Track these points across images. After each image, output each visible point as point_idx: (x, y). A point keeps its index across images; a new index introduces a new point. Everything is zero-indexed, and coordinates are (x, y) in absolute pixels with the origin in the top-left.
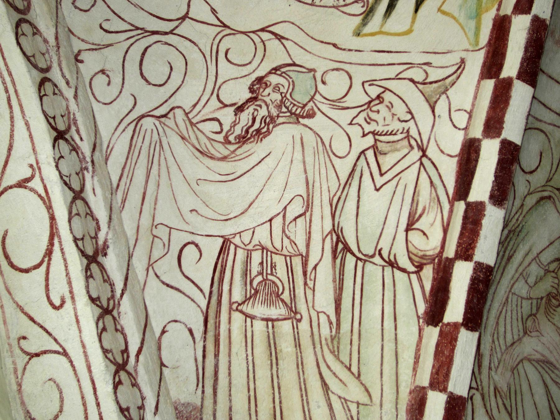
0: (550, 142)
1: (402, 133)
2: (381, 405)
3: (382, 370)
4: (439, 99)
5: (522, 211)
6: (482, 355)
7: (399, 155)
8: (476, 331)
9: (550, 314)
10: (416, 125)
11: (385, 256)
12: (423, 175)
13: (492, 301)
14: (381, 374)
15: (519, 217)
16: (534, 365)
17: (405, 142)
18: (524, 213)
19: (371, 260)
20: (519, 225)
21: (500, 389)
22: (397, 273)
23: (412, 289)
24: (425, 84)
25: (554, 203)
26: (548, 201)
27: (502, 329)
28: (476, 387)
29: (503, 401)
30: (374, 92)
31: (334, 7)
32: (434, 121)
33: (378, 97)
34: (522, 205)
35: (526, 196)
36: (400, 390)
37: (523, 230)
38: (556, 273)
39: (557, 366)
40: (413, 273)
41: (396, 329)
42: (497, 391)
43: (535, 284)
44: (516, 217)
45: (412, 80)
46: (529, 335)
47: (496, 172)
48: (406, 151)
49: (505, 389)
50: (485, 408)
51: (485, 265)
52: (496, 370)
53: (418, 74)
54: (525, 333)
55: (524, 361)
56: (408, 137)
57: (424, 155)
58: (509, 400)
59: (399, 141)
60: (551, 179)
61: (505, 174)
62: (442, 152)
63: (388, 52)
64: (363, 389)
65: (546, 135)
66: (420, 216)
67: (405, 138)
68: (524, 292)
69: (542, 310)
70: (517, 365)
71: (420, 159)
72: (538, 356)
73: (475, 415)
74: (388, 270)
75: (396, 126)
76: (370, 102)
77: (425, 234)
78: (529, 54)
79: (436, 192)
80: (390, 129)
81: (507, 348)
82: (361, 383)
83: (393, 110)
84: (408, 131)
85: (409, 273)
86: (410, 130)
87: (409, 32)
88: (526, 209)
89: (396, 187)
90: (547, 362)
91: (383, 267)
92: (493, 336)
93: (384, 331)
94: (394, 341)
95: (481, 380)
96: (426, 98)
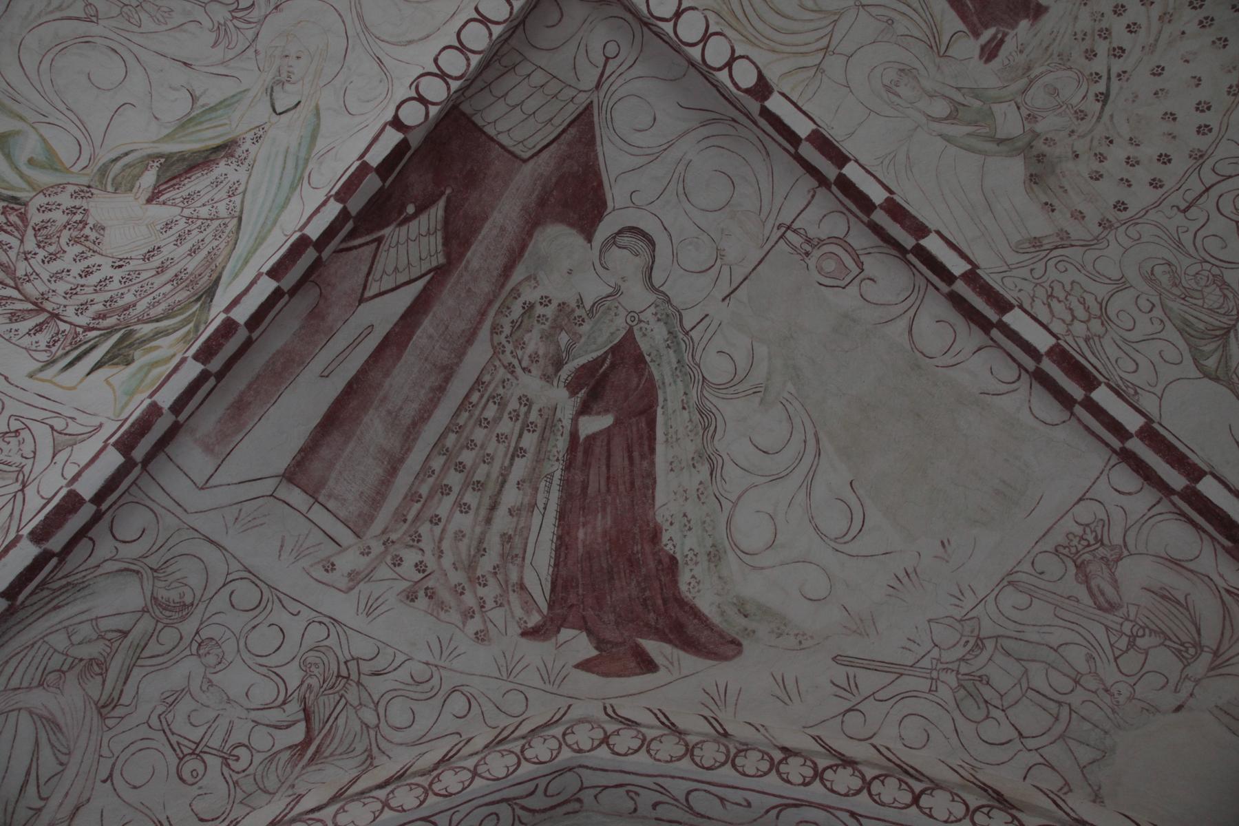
0: (158, 523)
9: (84, 677)
18: (96, 574)
20: (83, 582)
24: (60, 433)
26: (135, 575)
30: (15, 425)
31: (26, 349)
33: (17, 431)
34: (98, 566)
35: (107, 560)
38: (112, 643)
39: (64, 729)
43: (79, 644)
44: (84, 573)
45: (52, 427)
46: (44, 688)
47: (48, 514)
48: (11, 482)
53: (59, 424)
54: (40, 684)
56: (21, 471)
57: (22, 491)
62: (38, 492)
63: (47, 398)
65: (156, 516)
68: (61, 647)
72: (46, 713)
75: (17, 459)
76: (7, 433)
78: (133, 430)
79: (10, 523)
80: (9, 460)
83: (21, 447)
84: (23, 467)
87: (74, 388)
88: (100, 571)
90: (53, 722)
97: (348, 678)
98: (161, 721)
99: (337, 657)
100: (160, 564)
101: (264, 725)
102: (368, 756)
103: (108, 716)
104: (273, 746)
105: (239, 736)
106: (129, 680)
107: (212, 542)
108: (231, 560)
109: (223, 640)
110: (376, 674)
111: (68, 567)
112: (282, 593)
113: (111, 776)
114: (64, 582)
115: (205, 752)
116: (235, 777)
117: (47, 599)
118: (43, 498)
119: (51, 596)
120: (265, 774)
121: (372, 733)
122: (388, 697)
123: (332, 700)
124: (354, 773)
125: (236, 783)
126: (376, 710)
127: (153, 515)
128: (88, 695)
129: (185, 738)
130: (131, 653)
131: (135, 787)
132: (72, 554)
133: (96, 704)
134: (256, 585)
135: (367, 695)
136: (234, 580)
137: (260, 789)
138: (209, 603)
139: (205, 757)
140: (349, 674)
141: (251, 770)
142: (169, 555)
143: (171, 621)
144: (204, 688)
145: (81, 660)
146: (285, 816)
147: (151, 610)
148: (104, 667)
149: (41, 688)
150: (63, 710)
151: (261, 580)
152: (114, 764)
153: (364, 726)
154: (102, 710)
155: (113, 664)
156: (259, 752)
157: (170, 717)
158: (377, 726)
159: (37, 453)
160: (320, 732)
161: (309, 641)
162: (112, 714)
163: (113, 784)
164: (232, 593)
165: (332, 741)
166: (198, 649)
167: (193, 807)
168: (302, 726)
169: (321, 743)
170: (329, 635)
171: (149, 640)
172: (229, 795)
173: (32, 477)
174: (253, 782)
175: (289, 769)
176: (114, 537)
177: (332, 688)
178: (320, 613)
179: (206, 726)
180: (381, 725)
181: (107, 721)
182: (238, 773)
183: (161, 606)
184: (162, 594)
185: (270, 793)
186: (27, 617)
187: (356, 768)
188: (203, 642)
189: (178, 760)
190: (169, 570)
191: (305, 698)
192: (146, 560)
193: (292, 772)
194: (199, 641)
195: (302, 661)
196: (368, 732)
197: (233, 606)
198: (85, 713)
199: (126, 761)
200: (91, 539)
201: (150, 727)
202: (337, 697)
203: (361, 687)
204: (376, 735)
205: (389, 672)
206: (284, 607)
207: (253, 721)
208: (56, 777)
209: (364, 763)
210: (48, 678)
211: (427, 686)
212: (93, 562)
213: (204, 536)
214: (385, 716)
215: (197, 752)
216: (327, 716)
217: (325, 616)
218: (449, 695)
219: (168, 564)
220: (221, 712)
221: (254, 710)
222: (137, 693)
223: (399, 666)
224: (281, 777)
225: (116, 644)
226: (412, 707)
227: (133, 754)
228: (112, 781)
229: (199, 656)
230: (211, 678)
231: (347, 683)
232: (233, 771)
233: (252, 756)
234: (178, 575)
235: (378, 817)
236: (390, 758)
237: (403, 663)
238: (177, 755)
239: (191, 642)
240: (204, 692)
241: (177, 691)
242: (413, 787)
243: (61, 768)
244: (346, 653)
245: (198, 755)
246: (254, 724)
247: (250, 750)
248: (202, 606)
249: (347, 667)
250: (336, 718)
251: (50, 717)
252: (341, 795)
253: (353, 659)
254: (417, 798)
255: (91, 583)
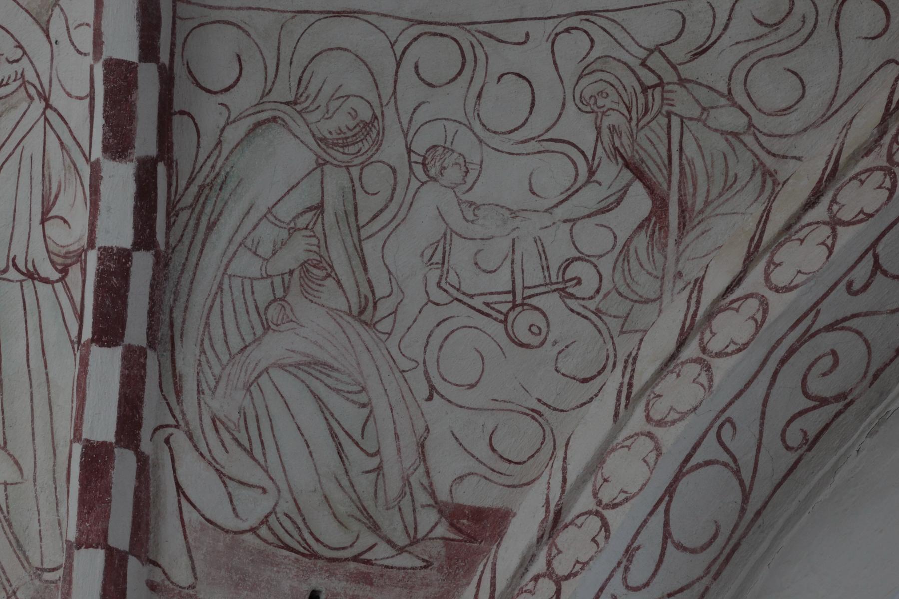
0: (249, 35)
1: (15, 81)
2: (35, 480)
3: (33, 429)
4: (52, 15)
5: (220, 152)
6: (180, 376)
7: (16, 115)
8: (117, 345)
9: (310, 290)
10: (32, 62)
11: (21, 265)
12: (51, 136)
13: (189, 295)
14: (33, 434)
15: (216, 161)
16: (290, 373)
17: (22, 93)
19: (4, 276)
20: (218, 174)
21: (223, 419)
22: (40, 285)
23: (60, 304)
25: (285, 125)
26: (273, 125)
27: (217, 331)
28: (174, 423)
29: (232, 435)
32: (52, 51)
34: (219, 142)
36: (57, 452)
37: (228, 180)
39: (336, 365)
40: (57, 281)
41: (46, 367)
42: (218, 422)
43: (273, 254)
46: (274, 331)
47: (105, 111)
48: (25, 105)
49: (235, 416)
50: (197, 450)
51: (115, 249)
52: (213, 393)
54: (266, 329)
55: (270, 371)
56: (25, 83)
57: (48, 106)
58: (243, 431)
59: (14, 92)
60: (270, 91)
61: (120, 110)
62: (69, 95)
64: (12, 462)
65: (239, 27)
66: (57, 197)
67: (21, 86)
68: (254, 271)
69: (295, 288)
70: (259, 376)
71: (44, 113)
72: (297, 358)
73: (177, 464)
74: (28, 284)
77: (65, 221)
79: (70, 156)
81: (232, 357)
82: (9, 454)
84: (23, 75)
85: (52, 282)
86: (25, 73)
88: (226, 149)
89: (20, 163)
90: (315, 364)
91: (21, 281)
92: (202, 345)
93: (32, 373)
94: (45, 385)
95: (182, 412)
96: (34, 19)
97: (661, 84)
98: (444, 290)
99: (625, 64)
100: (294, 89)
101: (584, 217)
102: (763, 175)
103: (375, 320)
104: (615, 237)
105: (559, 251)
106: (367, 262)
107: (338, 14)
108: (384, 23)
109: (449, 139)
110: (701, 52)
111: (184, 168)
112: (486, 23)
113: (432, 388)
114: (194, 189)
115: (530, 297)
116: (592, 305)
117: (192, 223)
118: (81, 99)
119: (195, 216)
120: (629, 280)
121: (749, 139)
122: (739, 75)
123: (658, 129)
124: (758, 210)
125: (598, 313)
126: (734, 104)
127: (235, 29)
128: (332, 310)
129: (492, 293)
130: (344, 228)
131: (472, 386)
132: (175, 148)
133: (350, 314)
134: (441, 35)
135: (706, 90)
136: (406, 49)
137: (636, 302)
138: (395, 102)
139: (534, 301)
140: (660, 78)
141: (607, 285)
142: (296, 72)
143: (365, 157)
144: (471, 217)
145: (291, 272)
146: (695, 315)
147: (328, 158)
148: (325, 265)
149: (271, 331)
150: (315, 343)
151: (443, 24)
152: (426, 373)
153: (729, 137)
154: (363, 318)
155: (334, 255)
156: (601, 256)
157: (452, 278)
158: (751, 125)
159: (23, 44)
160: (670, 182)
161: (570, 70)
162: (379, 314)
163: (442, 396)
164: (416, 67)
165: (695, 185)
166: (426, 171)
167: (563, 371)
168: (638, 188)
169: (680, 195)
170: (592, 41)
171: (354, 198)
172: (600, 332)
173: (45, 81)
174: (620, 298)
175: (658, 256)
176: (208, 91)
177: (646, 111)
178: (559, 16)
179: (508, 262)
180: (754, 122)
181: (378, 327)
182: (591, 298)
183: (337, 145)
184: (327, 128)
185: (655, 300)
186: (187, 259)
187: (755, 200)
188: (425, 158)
189: (502, 326)
190: (312, 90)
191: (616, 149)
192: (273, 96)
193: (666, 257)
194: (420, 160)
195: (578, 101)
196: (742, 141)
197: (430, 85)
198: (344, 332)
199: (438, 362)
200: (182, 113)
201: (437, 305)
202: (664, 121)
203: (688, 85)
204: (757, 139)
205: (719, 38)
206: (502, 42)
207: (565, 221)
208: (368, 423)
209: (763, 187)
210: (269, 317)
211: (793, 22)
212: (208, 142)
213: (321, 13)
214: (754, 104)
215: (519, 301)
216: (665, 154)
217: (569, 16)
218: (838, 13)
219: (304, 83)
220: (515, 234)
221: (556, 206)
222: (389, 272)
223: (729, 19)
224: (655, 273)
225: (318, 227)
226: (789, 66)
227: (441, 347)
228: (438, 393)
229: (435, 180)
230: (471, 199)
231: (663, 91)
232: (584, 299)
233: (596, 266)
234: (328, 90)
235: (833, 245)
236: (799, 159)
237: (732, 10)
238: (496, 319)
239: (410, 168)
240: (473, 222)
241: (438, 241)
242: (863, 177)
243: (366, 411)
244: (635, 49)
245: (523, 305)
246: (569, 225)
247: (586, 260)
248: (390, 112)
249: (650, 69)
250: (681, 150)
251: (308, 360)
252: (758, 246)
253: (651, 52)
254: (880, 187)
255: (228, 169)
